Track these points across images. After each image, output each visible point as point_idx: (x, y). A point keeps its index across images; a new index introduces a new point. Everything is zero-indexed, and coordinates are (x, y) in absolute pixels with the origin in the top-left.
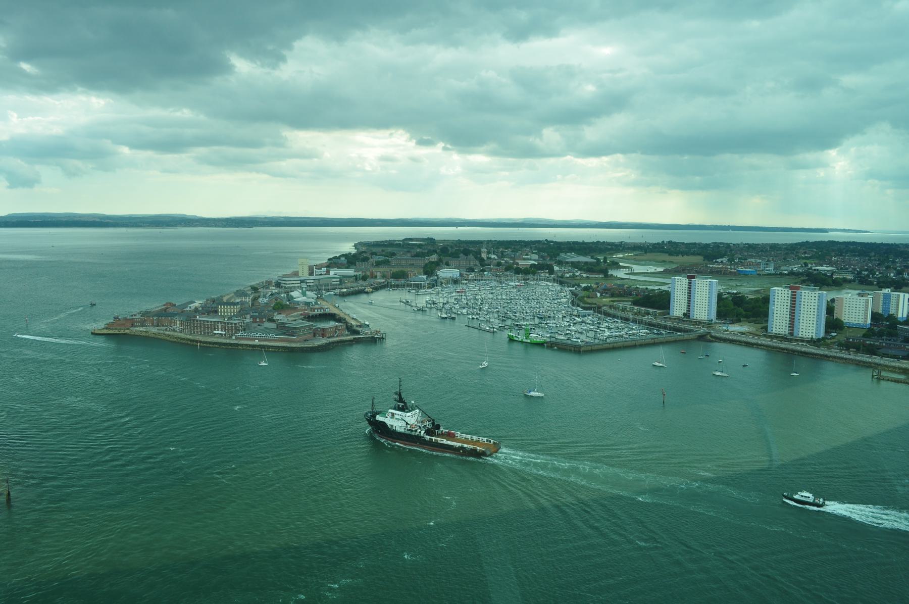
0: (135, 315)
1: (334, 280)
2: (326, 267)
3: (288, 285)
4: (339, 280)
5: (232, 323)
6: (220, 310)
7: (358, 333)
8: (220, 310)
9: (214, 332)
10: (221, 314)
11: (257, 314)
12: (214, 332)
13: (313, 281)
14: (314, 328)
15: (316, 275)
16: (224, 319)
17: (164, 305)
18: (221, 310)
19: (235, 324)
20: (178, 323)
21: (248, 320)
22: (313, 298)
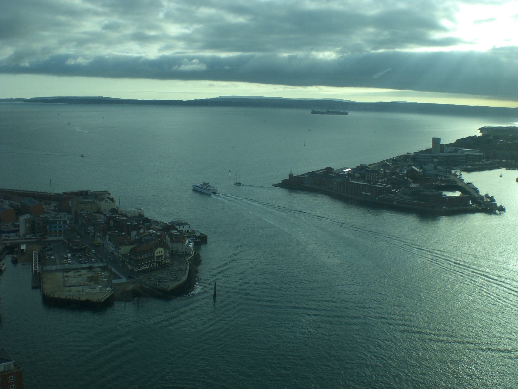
0: (303, 175)
1: (460, 158)
2: (455, 146)
3: (422, 160)
4: (465, 158)
5: (377, 187)
6: (367, 176)
7: (480, 204)
8: (367, 176)
9: (362, 193)
10: (368, 179)
11: (397, 181)
12: (362, 193)
13: (443, 157)
14: (443, 197)
15: (446, 153)
16: (371, 184)
17: (325, 169)
18: (368, 176)
19: (379, 188)
20: (335, 183)
21: (389, 186)
22: (443, 172)
